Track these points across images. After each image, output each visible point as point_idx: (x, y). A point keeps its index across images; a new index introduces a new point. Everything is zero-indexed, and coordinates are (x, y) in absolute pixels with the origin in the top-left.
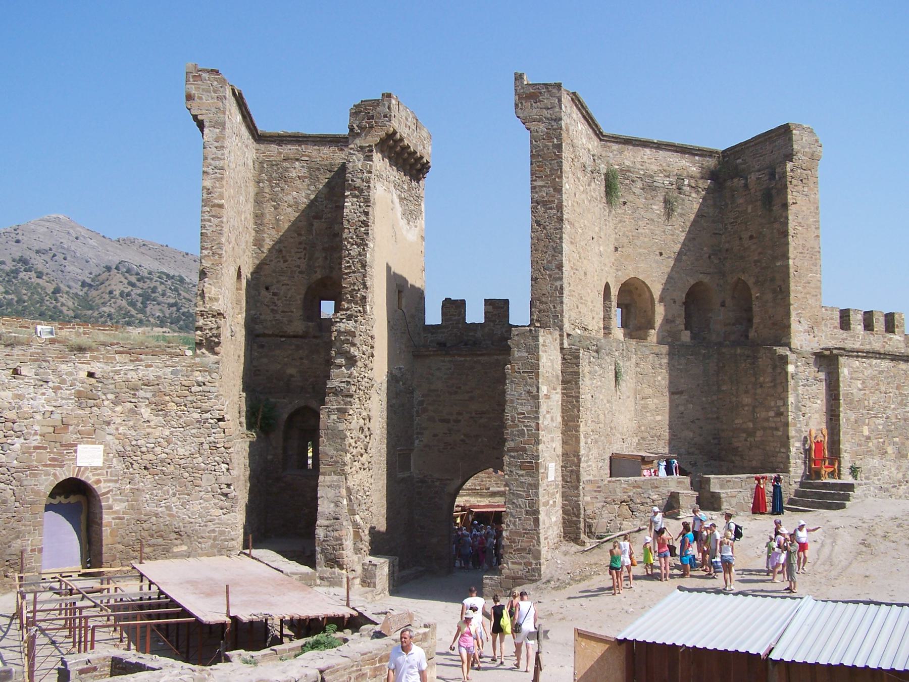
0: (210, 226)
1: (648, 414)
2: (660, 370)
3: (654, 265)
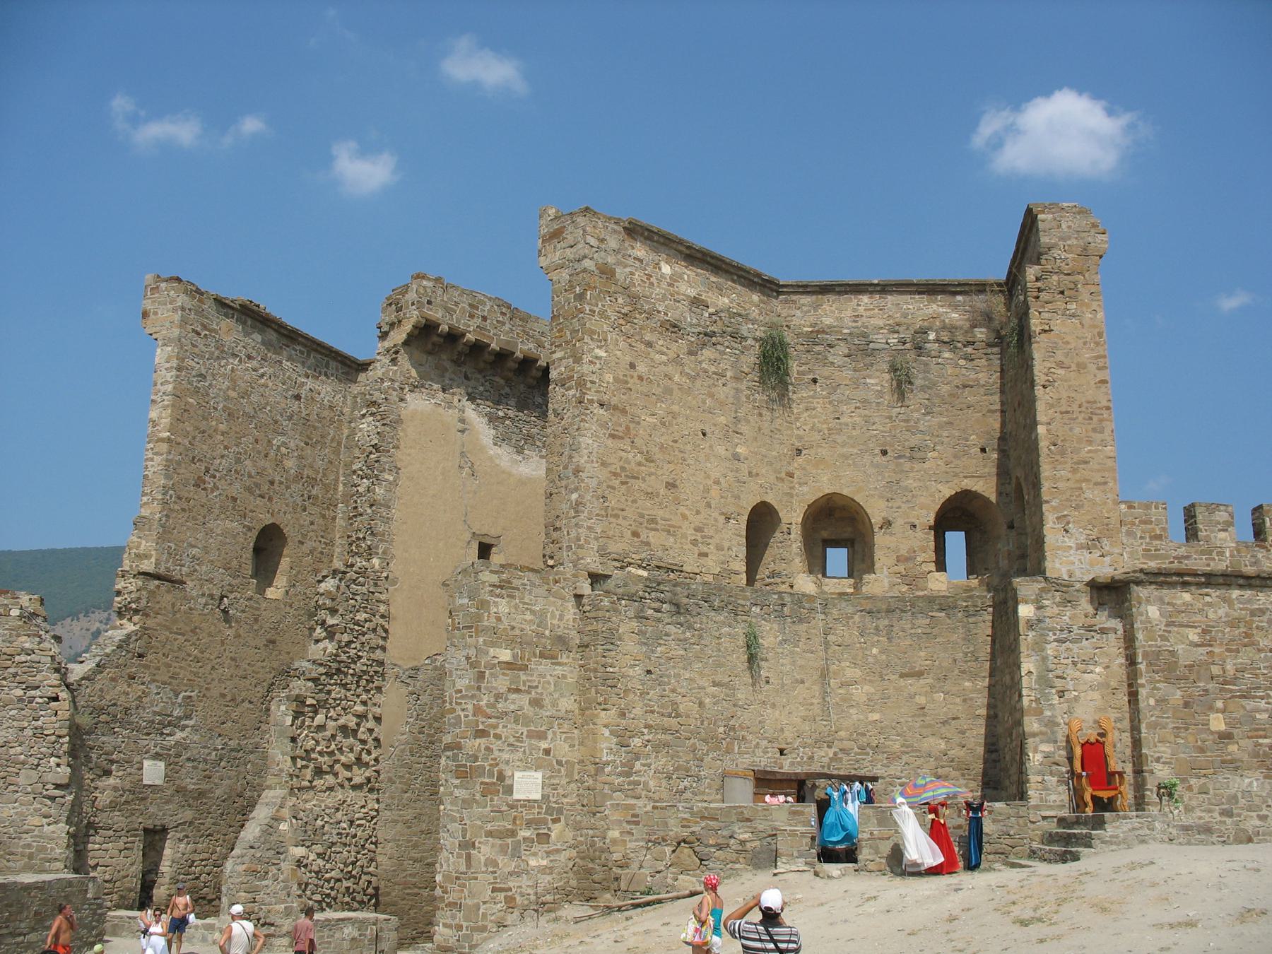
0: (153, 466)
1: (852, 711)
2: (876, 638)
3: (871, 471)
